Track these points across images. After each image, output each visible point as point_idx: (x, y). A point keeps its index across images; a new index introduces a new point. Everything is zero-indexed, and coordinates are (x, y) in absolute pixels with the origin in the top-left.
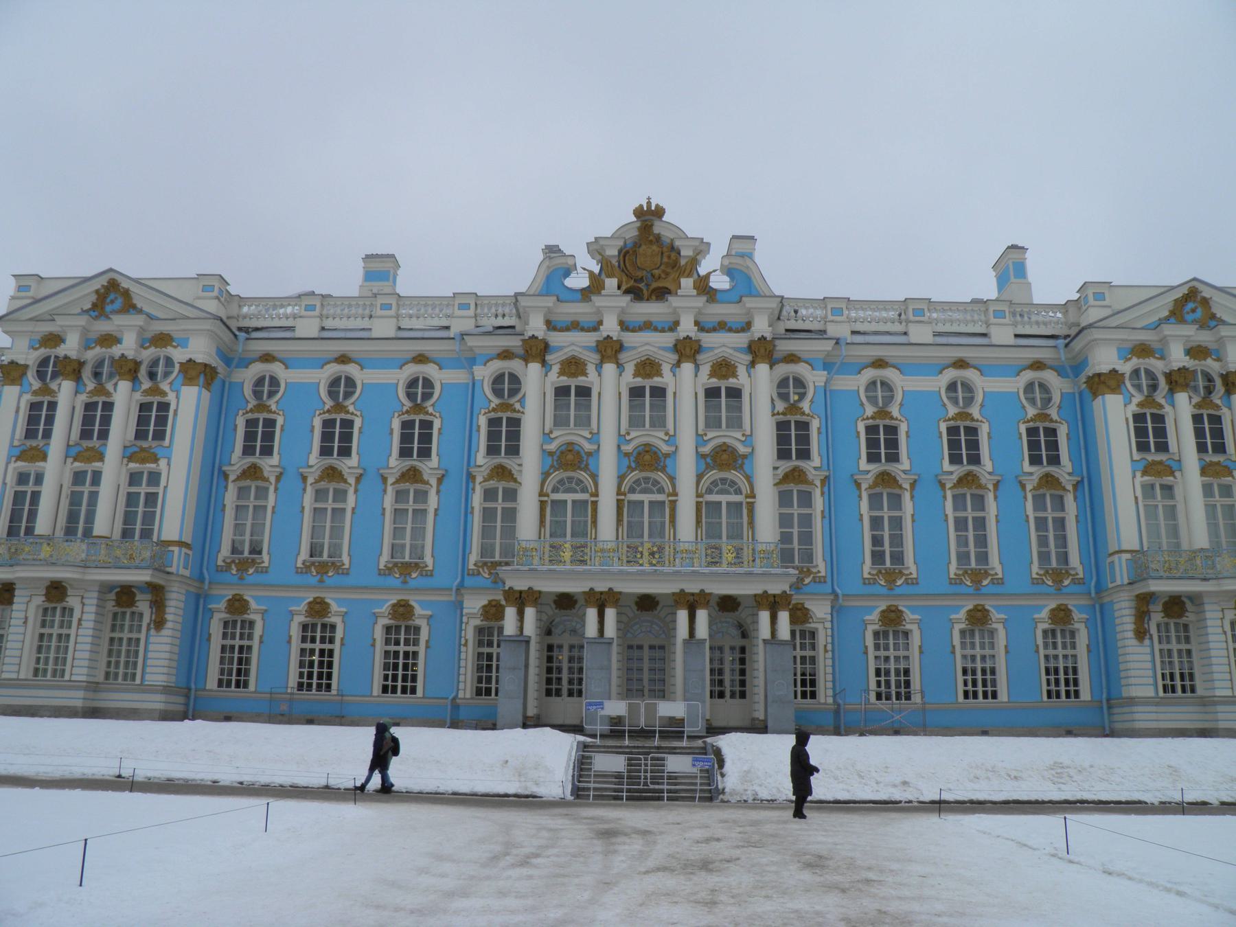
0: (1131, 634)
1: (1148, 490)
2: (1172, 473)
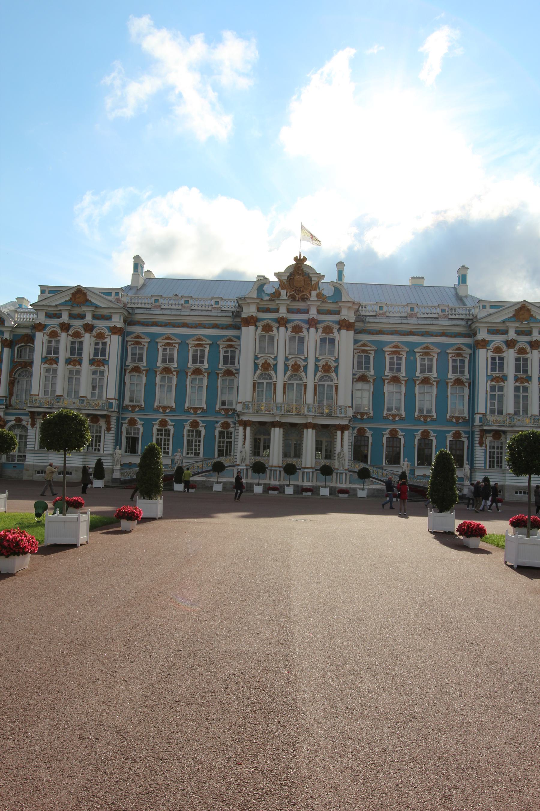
0: (478, 445)
1: (493, 388)
2: (503, 381)
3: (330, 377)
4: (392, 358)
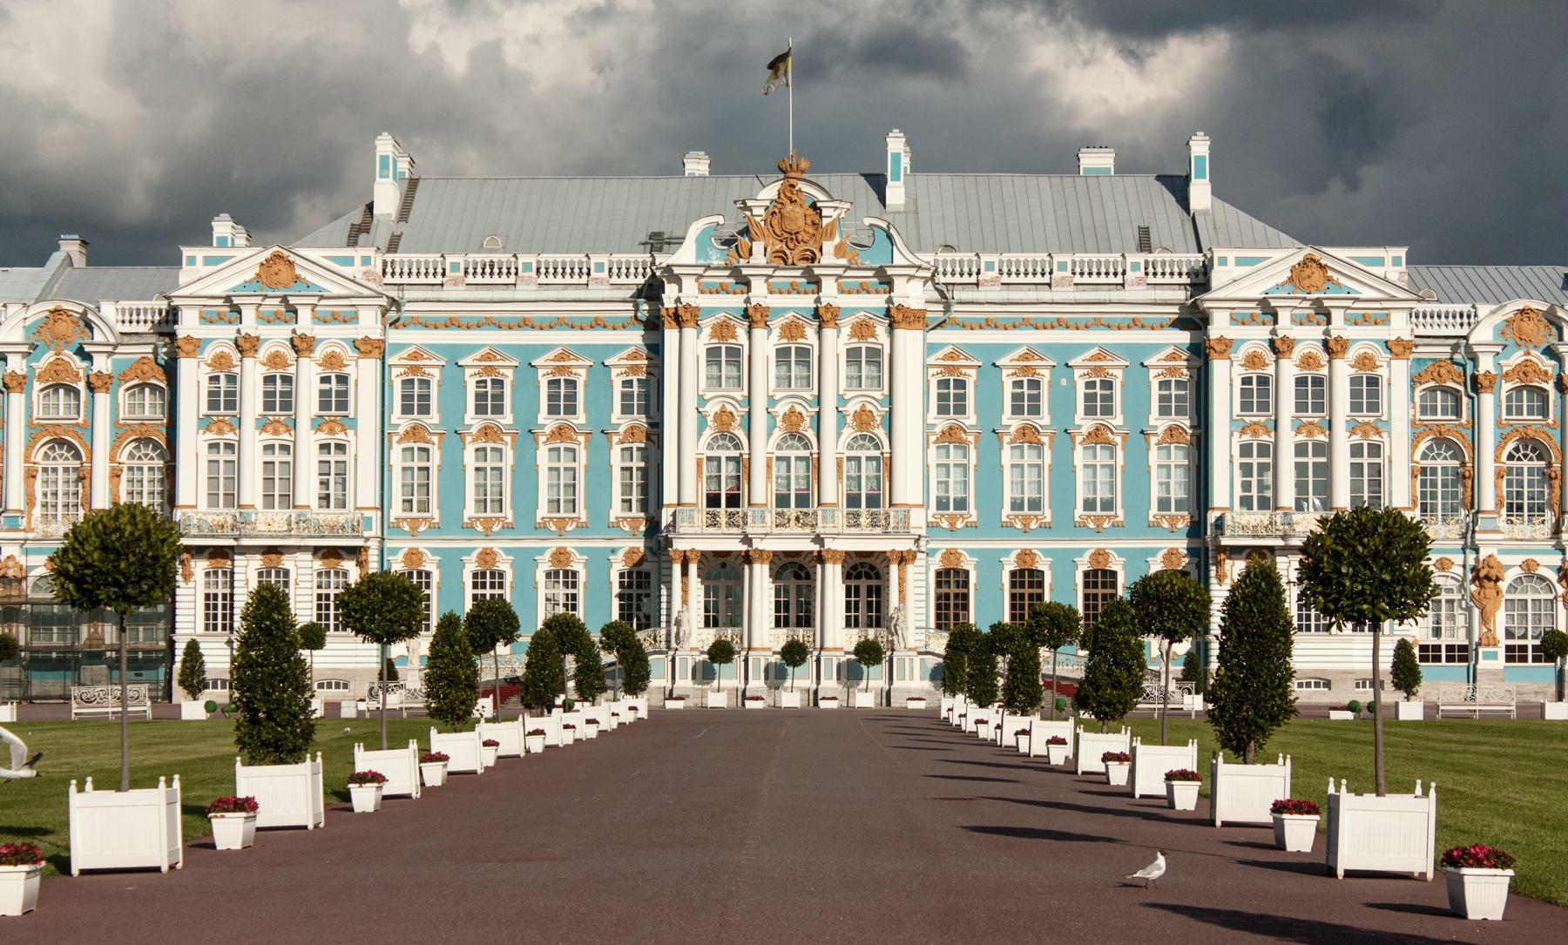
1: (1246, 450)
3: (872, 439)
4: (1018, 384)
